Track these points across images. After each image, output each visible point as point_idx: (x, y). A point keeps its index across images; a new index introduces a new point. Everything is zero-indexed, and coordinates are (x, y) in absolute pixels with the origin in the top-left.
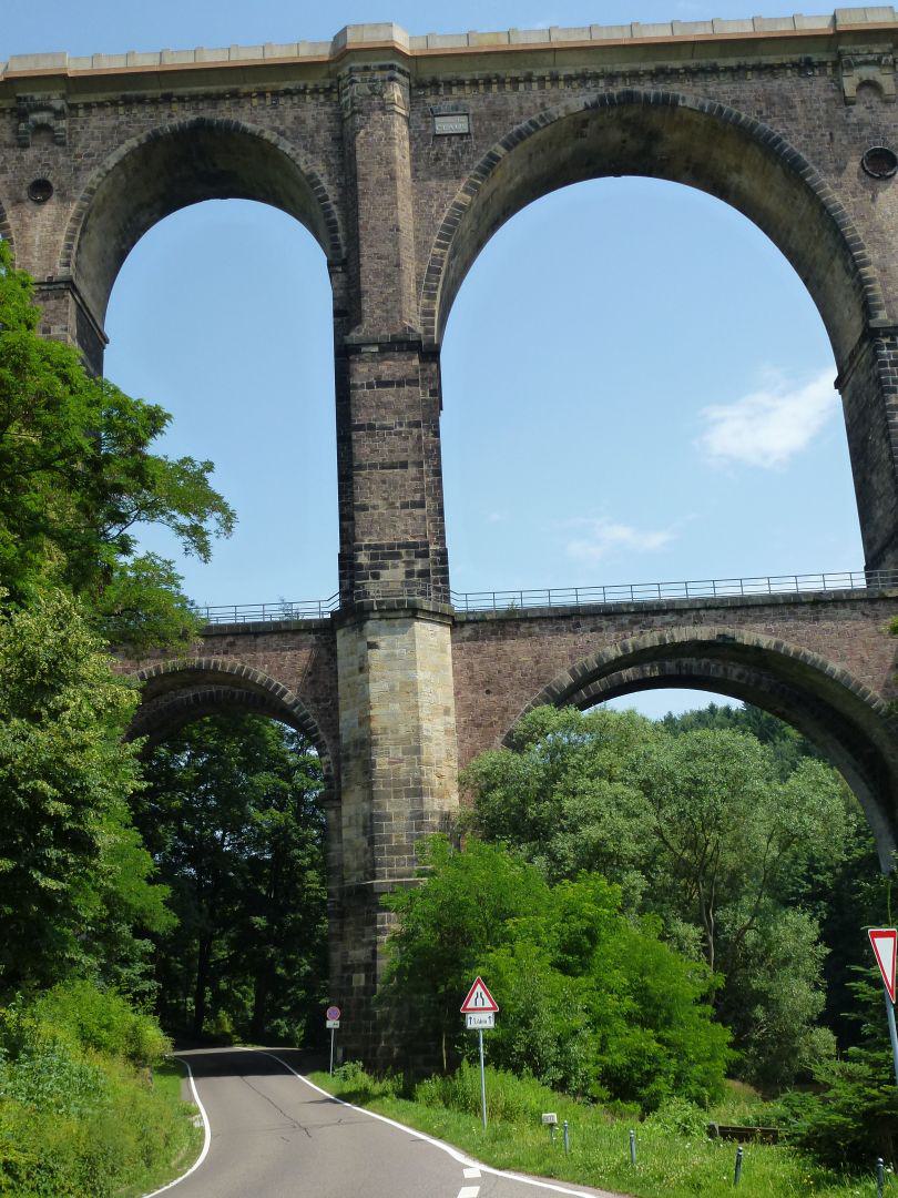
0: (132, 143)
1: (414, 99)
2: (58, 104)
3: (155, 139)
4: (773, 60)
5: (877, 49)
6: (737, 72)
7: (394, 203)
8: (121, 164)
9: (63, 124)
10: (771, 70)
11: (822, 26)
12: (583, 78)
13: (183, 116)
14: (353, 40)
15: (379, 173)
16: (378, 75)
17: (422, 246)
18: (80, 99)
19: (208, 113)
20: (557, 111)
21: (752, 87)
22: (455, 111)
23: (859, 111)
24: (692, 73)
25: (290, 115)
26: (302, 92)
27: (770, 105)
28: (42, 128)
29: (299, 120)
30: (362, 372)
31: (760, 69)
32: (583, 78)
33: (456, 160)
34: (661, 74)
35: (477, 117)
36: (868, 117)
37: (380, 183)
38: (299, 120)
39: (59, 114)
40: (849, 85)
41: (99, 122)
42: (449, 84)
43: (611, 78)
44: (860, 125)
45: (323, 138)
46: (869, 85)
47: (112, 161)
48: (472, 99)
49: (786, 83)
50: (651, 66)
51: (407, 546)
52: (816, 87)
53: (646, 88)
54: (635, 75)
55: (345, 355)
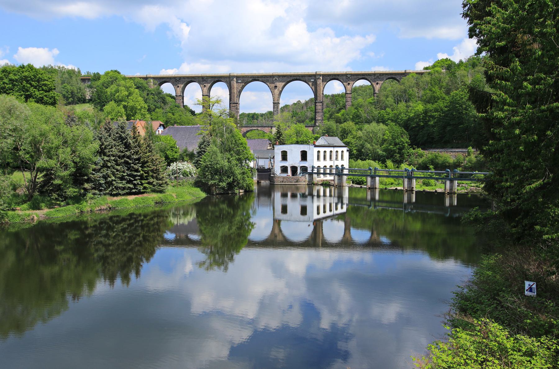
1: (236, 79)
6: (265, 77)
10: (268, 77)
11: (272, 74)
14: (231, 74)
17: (237, 93)
19: (219, 79)
30: (231, 105)
31: (267, 77)
35: (242, 81)
40: (274, 79)
41: (210, 79)
43: (254, 77)
52: (271, 79)
53: (256, 78)
54: (255, 77)
55: (230, 104)
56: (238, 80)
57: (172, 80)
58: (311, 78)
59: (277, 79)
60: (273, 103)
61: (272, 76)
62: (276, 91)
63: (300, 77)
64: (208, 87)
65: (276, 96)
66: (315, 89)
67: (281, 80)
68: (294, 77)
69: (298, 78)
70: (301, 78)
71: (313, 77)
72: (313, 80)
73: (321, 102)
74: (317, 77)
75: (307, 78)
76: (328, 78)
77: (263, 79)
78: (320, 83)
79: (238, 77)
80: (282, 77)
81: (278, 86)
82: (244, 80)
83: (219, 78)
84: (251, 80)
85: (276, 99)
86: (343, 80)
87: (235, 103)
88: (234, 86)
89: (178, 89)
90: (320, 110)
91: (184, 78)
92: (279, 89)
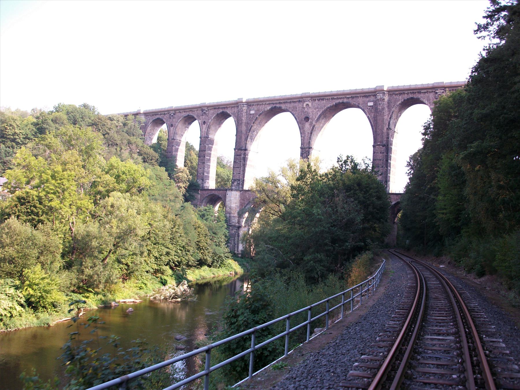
0: (215, 115)
2: (206, 109)
3: (218, 114)
4: (295, 100)
5: (309, 99)
6: (290, 102)
7: (241, 127)
8: (214, 118)
9: (207, 112)
12: (269, 104)
13: (221, 111)
15: (240, 122)
16: (242, 106)
18: (209, 108)
19: (224, 110)
20: (266, 110)
21: (292, 104)
22: (253, 110)
23: (306, 109)
24: (284, 103)
25: (233, 110)
26: (234, 107)
27: (294, 108)
28: (205, 113)
29: (234, 111)
32: (269, 104)
33: (252, 118)
34: (280, 103)
35: (256, 111)
36: (307, 110)
37: (241, 124)
38: (234, 111)
39: (206, 111)
41: (212, 111)
42: (253, 105)
43: (273, 104)
44: (306, 112)
45: (237, 114)
46: (307, 105)
47: (212, 118)
48: (255, 108)
49: (297, 104)
50: (278, 102)
51: (237, 179)
53: (278, 106)
56: (250, 110)
57: (166, 115)
58: (368, 99)
59: (310, 104)
60: (301, 148)
61: (301, 99)
62: (307, 125)
63: (348, 98)
64: (208, 124)
65: (307, 135)
66: (374, 121)
67: (316, 107)
68: (338, 98)
69: (345, 100)
70: (350, 101)
71: (372, 98)
72: (371, 104)
73: (383, 146)
74: (379, 97)
75: (361, 100)
76: (400, 97)
77: (288, 105)
78: (383, 109)
79: (250, 104)
80: (319, 100)
81: (311, 117)
82: (258, 110)
83: (225, 108)
84: (269, 108)
85: (306, 141)
86: (428, 100)
87: (241, 150)
88: (242, 120)
89: (172, 128)
90: (380, 162)
91: (180, 112)
92: (311, 124)
